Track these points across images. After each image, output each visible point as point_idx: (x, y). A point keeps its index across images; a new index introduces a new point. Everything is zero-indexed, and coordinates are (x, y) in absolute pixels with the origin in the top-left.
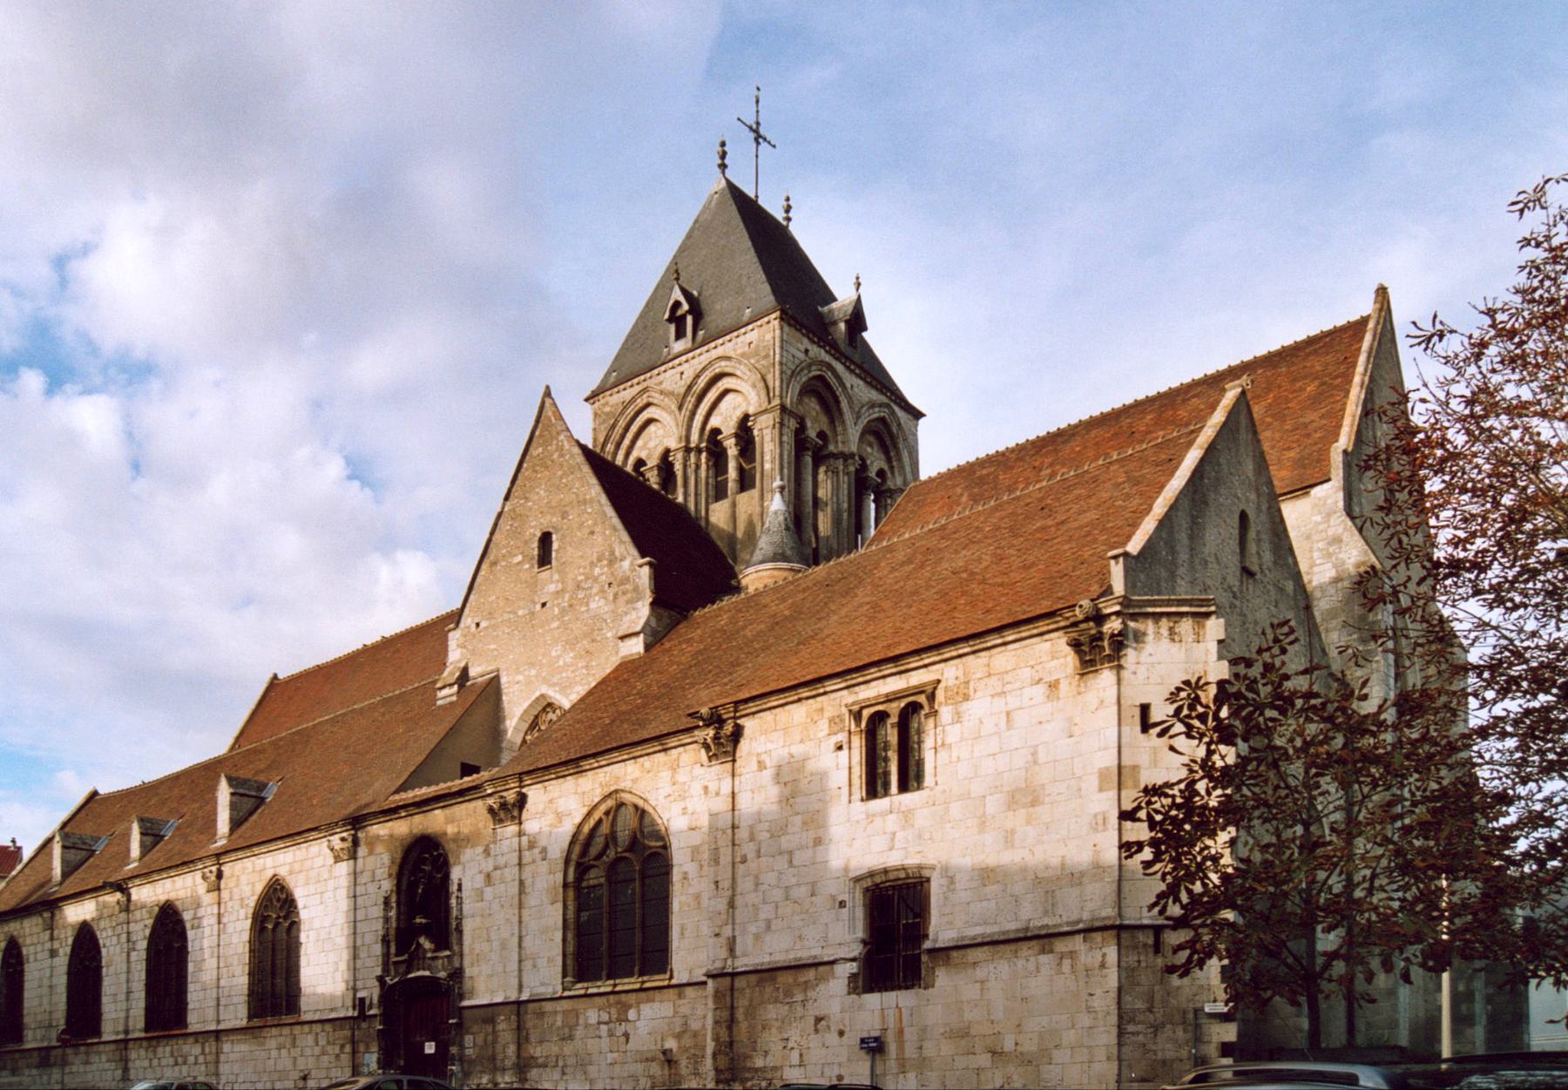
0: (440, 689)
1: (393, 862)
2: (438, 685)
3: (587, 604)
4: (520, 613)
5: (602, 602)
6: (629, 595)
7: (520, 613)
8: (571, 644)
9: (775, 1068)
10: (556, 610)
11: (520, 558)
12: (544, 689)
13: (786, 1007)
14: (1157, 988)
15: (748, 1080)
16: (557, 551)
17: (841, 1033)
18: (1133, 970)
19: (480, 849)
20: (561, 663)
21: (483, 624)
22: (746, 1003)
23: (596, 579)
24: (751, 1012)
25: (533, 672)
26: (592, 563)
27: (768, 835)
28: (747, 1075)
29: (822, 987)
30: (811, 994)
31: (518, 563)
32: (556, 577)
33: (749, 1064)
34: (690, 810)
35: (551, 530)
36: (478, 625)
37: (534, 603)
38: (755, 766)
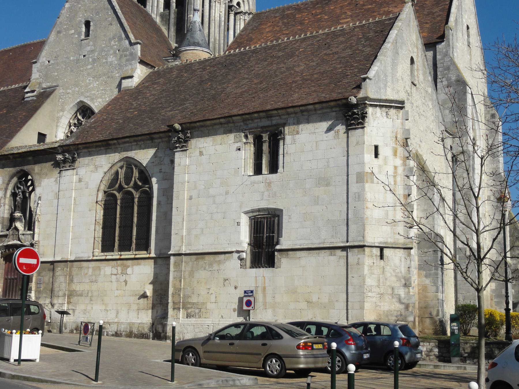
1: (3, 183)
2: (26, 91)
3: (106, 59)
4: (72, 58)
5: (114, 59)
6: (128, 57)
7: (72, 58)
8: (96, 77)
9: (203, 303)
10: (91, 60)
11: (73, 31)
12: (83, 99)
13: (210, 273)
14: (381, 276)
15: (189, 308)
16: (93, 30)
17: (236, 288)
18: (371, 266)
19: (53, 180)
21: (52, 62)
22: (190, 269)
23: (112, 47)
24: (192, 274)
25: (77, 89)
26: (110, 39)
27: (203, 187)
28: (189, 306)
29: (227, 263)
30: (222, 267)
32: (91, 43)
33: (190, 300)
34: (163, 171)
35: (90, 20)
36: (49, 62)
37: (80, 55)
38: (197, 153)
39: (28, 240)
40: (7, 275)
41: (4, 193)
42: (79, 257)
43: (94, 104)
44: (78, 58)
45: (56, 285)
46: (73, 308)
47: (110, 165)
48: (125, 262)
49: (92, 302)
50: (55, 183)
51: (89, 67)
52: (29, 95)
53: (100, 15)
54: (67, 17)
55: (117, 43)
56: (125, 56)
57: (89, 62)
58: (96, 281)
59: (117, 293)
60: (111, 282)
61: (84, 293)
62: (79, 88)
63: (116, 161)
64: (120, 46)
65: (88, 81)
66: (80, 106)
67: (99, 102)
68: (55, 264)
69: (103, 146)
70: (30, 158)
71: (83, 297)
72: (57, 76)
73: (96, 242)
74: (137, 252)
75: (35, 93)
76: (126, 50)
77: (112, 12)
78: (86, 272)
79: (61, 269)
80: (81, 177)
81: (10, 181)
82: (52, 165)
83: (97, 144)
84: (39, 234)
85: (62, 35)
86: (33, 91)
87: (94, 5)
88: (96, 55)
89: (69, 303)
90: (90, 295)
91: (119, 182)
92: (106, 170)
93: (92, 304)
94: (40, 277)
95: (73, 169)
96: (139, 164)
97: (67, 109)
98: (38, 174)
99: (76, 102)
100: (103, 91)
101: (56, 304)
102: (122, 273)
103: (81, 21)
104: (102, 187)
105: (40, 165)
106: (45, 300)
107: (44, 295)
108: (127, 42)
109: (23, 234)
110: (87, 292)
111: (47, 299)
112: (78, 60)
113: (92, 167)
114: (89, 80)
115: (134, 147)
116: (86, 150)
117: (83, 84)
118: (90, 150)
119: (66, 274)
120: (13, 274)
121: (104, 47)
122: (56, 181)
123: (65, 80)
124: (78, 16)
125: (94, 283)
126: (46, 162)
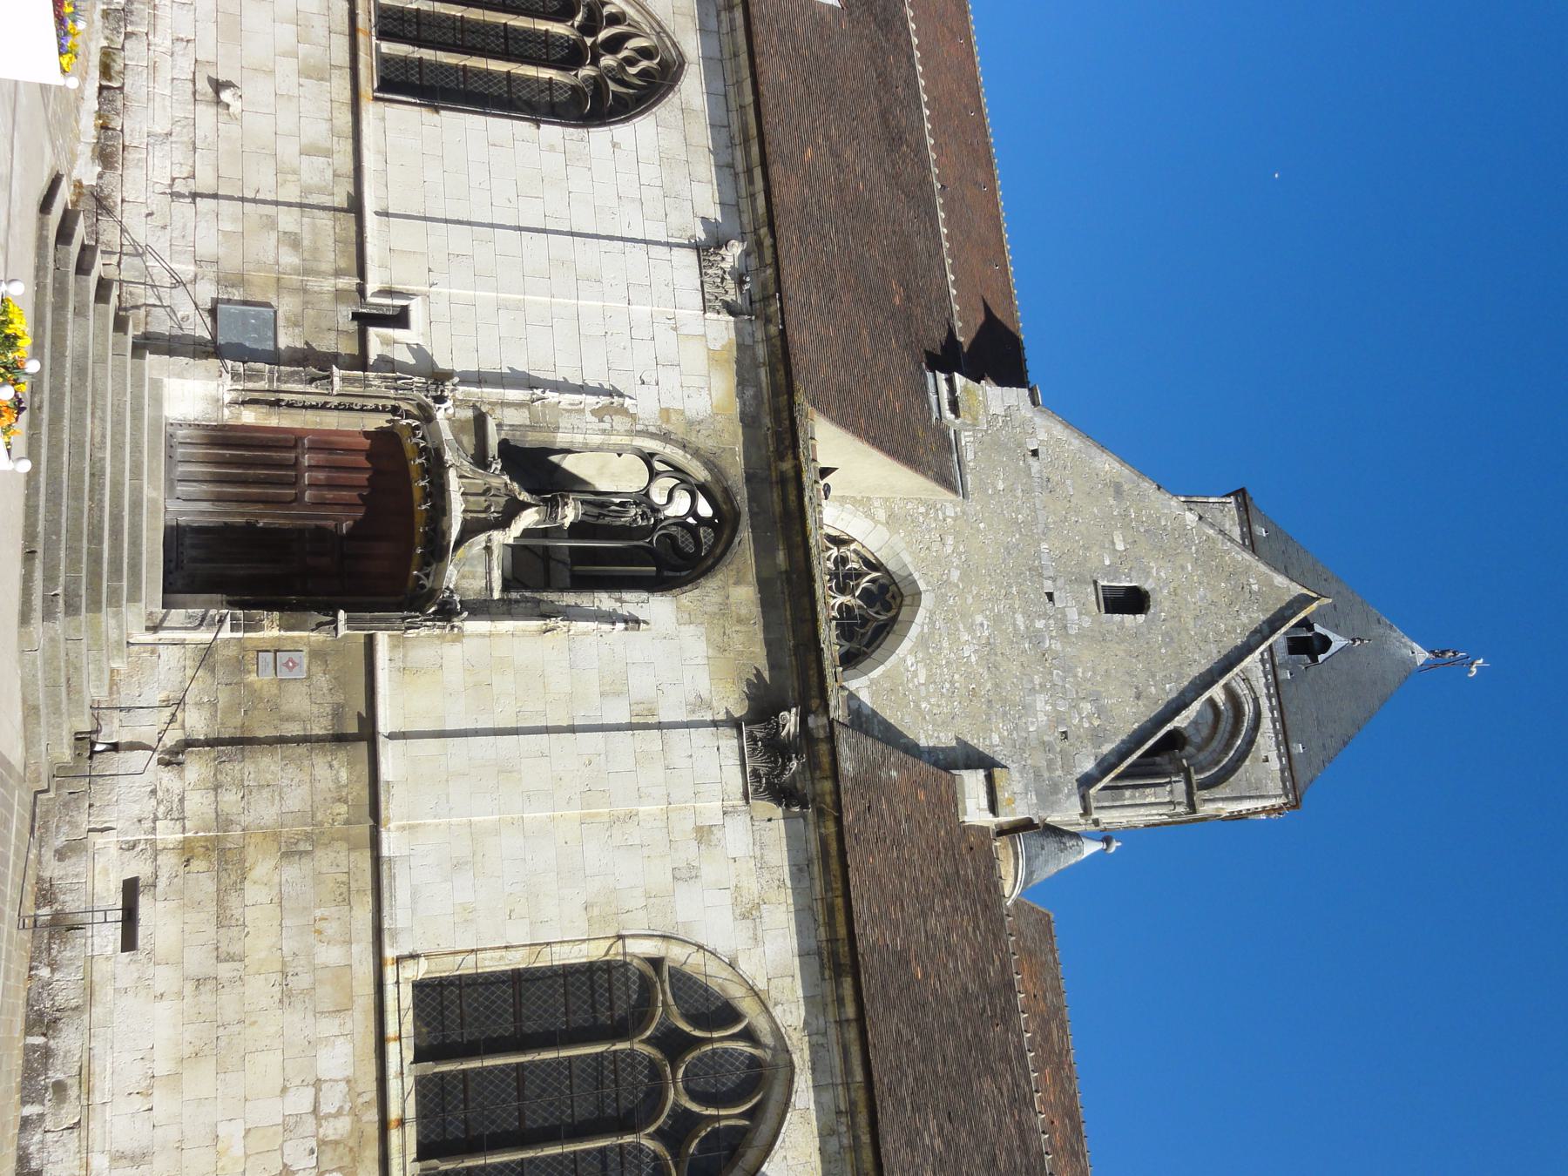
0: (950, 381)
1: (690, 423)
10: (1040, 624)
12: (927, 601)
16: (1122, 626)
20: (966, 637)
25: (955, 575)
31: (1113, 543)
32: (1087, 622)
35: (1152, 610)
36: (1035, 453)
37: (1054, 580)
39: (463, 577)
40: (314, 448)
41: (652, 429)
42: (392, 877)
43: (910, 651)
44: (1046, 574)
45: (267, 765)
46: (162, 883)
47: (761, 985)
48: (373, 1152)
49: (190, 987)
50: (692, 699)
51: (1020, 620)
52: (944, 387)
53: (1163, 651)
54: (1159, 519)
55: (1086, 725)
56: (1050, 763)
57: (1032, 621)
58: (286, 997)
59: (232, 1133)
60: (284, 1090)
61: (234, 932)
62: (958, 586)
63: (777, 1012)
64: (1078, 737)
65: (979, 619)
66: (900, 585)
67: (915, 674)
68: (363, 747)
69: (833, 940)
70: (781, 556)
71: (211, 930)
72: (995, 488)
73: (459, 958)
74: (410, 1082)
75: (949, 415)
76: (1068, 762)
77: (1170, 697)
78: (331, 928)
79: (339, 787)
80: (717, 833)
81: (696, 453)
82: (758, 674)
83: (840, 918)
85: (1112, 502)
86: (954, 406)
87: (1191, 624)
88: (1057, 646)
89: (187, 852)
90: (225, 970)
91: (711, 1112)
92: (744, 966)
93: (180, 995)
94: (305, 661)
95: (746, 796)
96: (765, 1129)
97: (896, 538)
98: (724, 609)
99: (916, 576)
100: (947, 685)
101: (181, 778)
102: (322, 1143)
103: (1148, 574)
104: (676, 954)
105: (756, 610)
106: (199, 704)
107: (223, 697)
108: (1088, 765)
109: (488, 549)
110: (235, 949)
111: (206, 713)
112: (1038, 573)
113: (752, 887)
114: (982, 625)
115: (827, 1097)
116: (814, 847)
117: (970, 600)
118: (816, 869)
119: (319, 816)
120: (321, 476)
121: (1075, 676)
122: (702, 703)
123: (982, 525)
124: (1161, 562)
125: (277, 988)
126: (769, 643)
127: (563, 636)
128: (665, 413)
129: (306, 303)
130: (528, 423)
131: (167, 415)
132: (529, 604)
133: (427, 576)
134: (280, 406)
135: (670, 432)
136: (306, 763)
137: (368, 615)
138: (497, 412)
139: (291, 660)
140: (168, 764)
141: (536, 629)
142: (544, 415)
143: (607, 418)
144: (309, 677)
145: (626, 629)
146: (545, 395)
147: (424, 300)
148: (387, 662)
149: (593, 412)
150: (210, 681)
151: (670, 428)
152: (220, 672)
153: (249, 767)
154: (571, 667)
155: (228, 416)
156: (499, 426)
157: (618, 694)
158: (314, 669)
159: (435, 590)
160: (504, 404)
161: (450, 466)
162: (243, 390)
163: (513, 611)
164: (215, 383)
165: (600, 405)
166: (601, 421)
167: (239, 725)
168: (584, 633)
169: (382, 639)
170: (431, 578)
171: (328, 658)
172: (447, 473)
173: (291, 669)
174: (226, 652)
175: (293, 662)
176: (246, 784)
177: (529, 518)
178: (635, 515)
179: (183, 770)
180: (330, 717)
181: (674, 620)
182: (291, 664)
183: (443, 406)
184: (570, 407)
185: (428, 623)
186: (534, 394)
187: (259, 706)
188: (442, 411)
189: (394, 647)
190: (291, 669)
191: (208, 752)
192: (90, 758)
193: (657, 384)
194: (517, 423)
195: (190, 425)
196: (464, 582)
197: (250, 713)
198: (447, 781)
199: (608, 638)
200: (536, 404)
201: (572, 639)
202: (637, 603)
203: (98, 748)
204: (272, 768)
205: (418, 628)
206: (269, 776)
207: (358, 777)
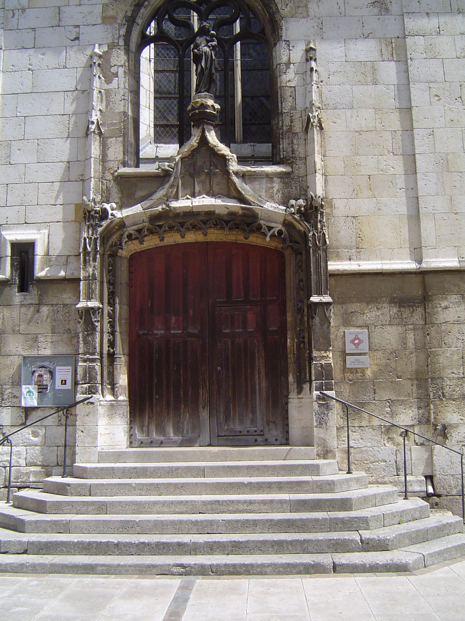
41: (123, 31)
50: (376, 10)
84: (324, 175)
94: (353, 330)
101: (457, 426)
106: (392, 414)
107: (386, 395)
109: (243, 176)
111: (401, 409)
127: (323, 114)
128: (106, 20)
129: (15, 332)
130: (121, 139)
131: (126, 446)
132: (295, 141)
133: (270, 228)
134: (114, 353)
135: (126, 16)
136: (443, 327)
137: (313, 277)
138: (111, 166)
139: (352, 342)
140: (445, 437)
141: (319, 136)
142: (113, 124)
143: (113, 70)
144: (367, 327)
145: (315, 60)
146: (95, 122)
147: (5, 229)
148: (352, 262)
149: (109, 81)
150: (373, 407)
151: (120, 16)
152: (366, 398)
153: (447, 373)
154: (352, 108)
155: (123, 397)
156: (125, 164)
157: (374, 70)
158: (360, 323)
159: (285, 220)
160: (104, 159)
161: (168, 206)
162: (102, 384)
163: (302, 155)
164: (100, 408)
165: (101, 76)
166: (116, 75)
167: (409, 382)
168: (321, 95)
169: (333, 266)
170: (272, 225)
171: (349, 311)
172: (175, 208)
173: (361, 341)
174: (346, 394)
175: (355, 339)
176: (462, 375)
177: (212, 137)
178: (209, 47)
179: (451, 425)
180: (402, 309)
181: (304, 20)
182: (356, 341)
183: (110, 212)
184: (104, 102)
185: (319, 226)
186: (94, 132)
187: (393, 366)
188: (114, 212)
189: (338, 257)
190: (361, 341)
191: (435, 406)
192: (439, 496)
193: (78, 26)
194: (122, 148)
195: (131, 428)
196: (276, 197)
197: (399, 374)
198: (456, 214)
199: (324, 75)
200: (103, 131)
201: (324, 107)
202: (290, 50)
203: (431, 490)
204: (448, 355)
205: (324, 234)
206: (456, 357)
207: (455, 285)
